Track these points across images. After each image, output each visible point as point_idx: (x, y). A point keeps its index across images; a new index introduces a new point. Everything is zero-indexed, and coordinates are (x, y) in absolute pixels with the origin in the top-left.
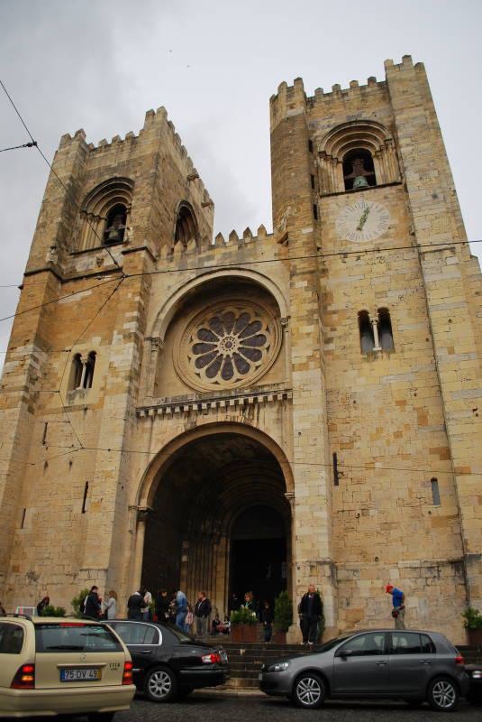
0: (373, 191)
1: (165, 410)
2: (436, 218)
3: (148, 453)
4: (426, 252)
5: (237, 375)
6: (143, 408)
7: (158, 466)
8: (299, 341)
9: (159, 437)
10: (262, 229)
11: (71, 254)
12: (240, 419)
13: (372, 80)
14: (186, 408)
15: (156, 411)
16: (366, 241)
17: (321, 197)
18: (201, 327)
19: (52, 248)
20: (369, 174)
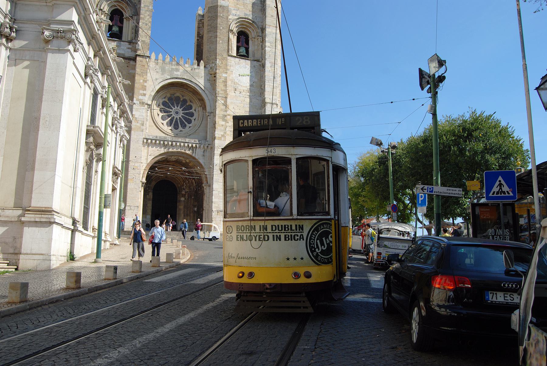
5: (180, 128)
6: (146, 139)
14: (166, 143)
15: (151, 142)
17: (229, 56)
18: (164, 100)
20: (246, 46)
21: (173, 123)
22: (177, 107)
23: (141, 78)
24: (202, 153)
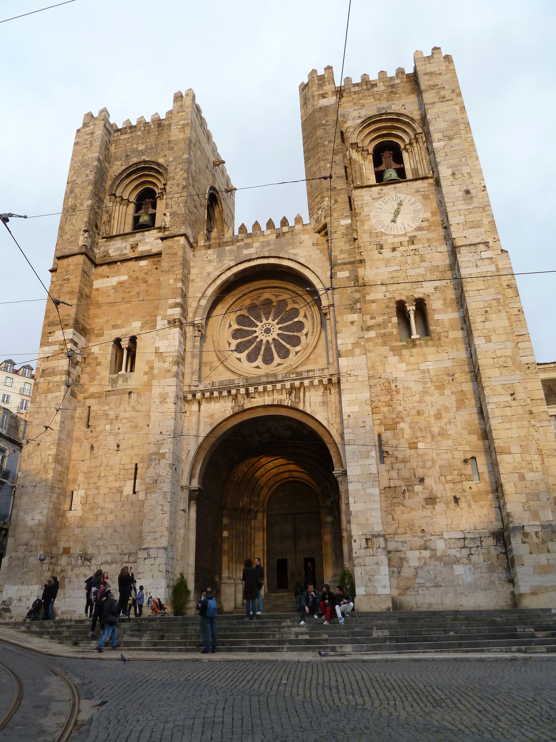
0: (405, 184)
1: (212, 394)
2: (470, 213)
3: (197, 436)
4: (461, 246)
5: (277, 359)
6: (191, 392)
7: (207, 447)
8: (344, 329)
9: (208, 420)
10: (298, 220)
11: (102, 238)
12: (287, 402)
13: (400, 72)
14: (234, 392)
15: (203, 395)
16: (401, 233)
17: (356, 188)
18: (239, 313)
19: (85, 231)
20: (398, 166)
21: (262, 352)
22: (267, 320)
23: (171, 276)
24: (319, 399)
